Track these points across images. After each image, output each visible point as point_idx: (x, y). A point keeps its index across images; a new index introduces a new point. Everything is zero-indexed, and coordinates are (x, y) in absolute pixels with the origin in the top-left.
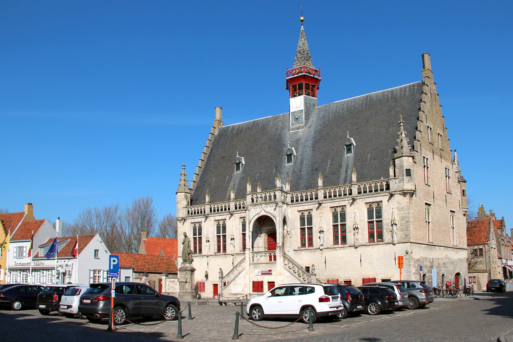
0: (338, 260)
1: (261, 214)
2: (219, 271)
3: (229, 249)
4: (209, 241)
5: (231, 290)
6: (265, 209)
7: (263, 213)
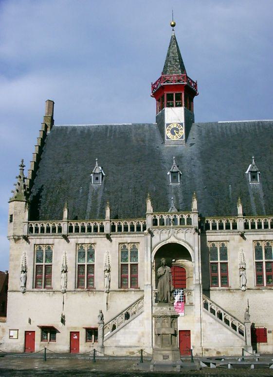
0: (266, 305)
1: (169, 241)
2: (99, 314)
3: (100, 281)
4: (66, 272)
5: (119, 341)
6: (176, 235)
7: (172, 240)
